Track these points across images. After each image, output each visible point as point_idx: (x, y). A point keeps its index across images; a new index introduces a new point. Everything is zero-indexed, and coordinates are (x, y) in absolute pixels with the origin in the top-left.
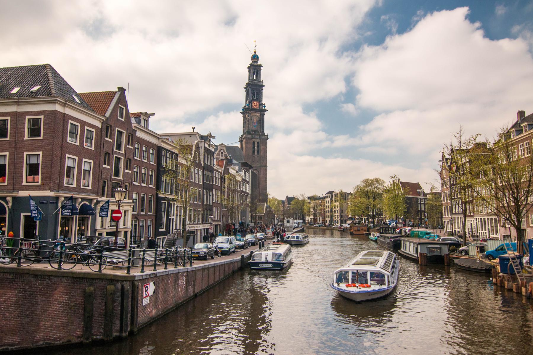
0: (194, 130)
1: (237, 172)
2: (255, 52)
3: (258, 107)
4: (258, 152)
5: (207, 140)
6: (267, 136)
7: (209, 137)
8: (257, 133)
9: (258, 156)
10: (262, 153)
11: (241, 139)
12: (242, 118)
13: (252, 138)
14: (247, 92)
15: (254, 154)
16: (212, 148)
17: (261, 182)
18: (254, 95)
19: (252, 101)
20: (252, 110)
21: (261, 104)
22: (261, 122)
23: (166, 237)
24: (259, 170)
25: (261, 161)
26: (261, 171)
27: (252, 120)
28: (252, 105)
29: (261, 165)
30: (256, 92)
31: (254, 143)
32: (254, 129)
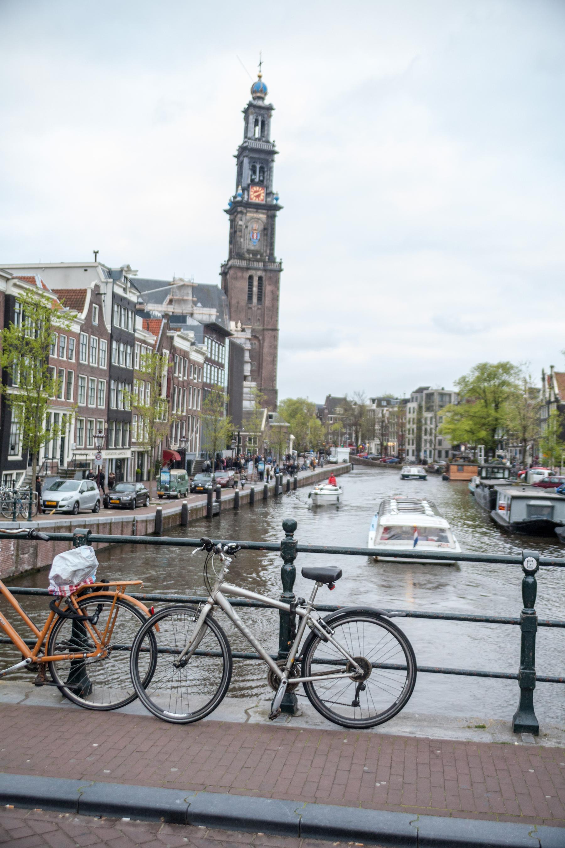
0: (96, 256)
1: (193, 344)
2: (260, 77)
3: (262, 200)
4: (260, 299)
5: (119, 279)
6: (280, 263)
7: (124, 273)
8: (259, 257)
9: (259, 307)
10: (267, 301)
11: (223, 269)
12: (228, 224)
13: (248, 269)
14: (240, 165)
15: (251, 303)
16: (131, 295)
17: (264, 364)
18: (254, 172)
19: (249, 185)
20: (249, 205)
21: (269, 194)
22: (269, 232)
23: (24, 471)
24: (261, 338)
25: (266, 319)
26: (264, 339)
27: (249, 228)
28: (248, 195)
29: (265, 327)
30: (258, 166)
31: (251, 278)
32: (252, 248)
